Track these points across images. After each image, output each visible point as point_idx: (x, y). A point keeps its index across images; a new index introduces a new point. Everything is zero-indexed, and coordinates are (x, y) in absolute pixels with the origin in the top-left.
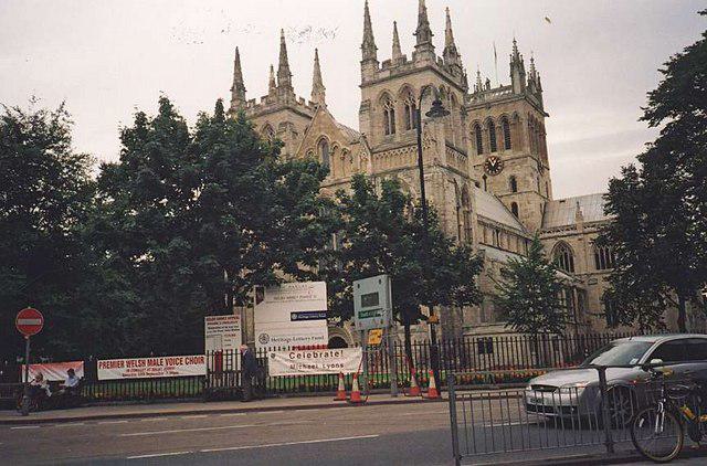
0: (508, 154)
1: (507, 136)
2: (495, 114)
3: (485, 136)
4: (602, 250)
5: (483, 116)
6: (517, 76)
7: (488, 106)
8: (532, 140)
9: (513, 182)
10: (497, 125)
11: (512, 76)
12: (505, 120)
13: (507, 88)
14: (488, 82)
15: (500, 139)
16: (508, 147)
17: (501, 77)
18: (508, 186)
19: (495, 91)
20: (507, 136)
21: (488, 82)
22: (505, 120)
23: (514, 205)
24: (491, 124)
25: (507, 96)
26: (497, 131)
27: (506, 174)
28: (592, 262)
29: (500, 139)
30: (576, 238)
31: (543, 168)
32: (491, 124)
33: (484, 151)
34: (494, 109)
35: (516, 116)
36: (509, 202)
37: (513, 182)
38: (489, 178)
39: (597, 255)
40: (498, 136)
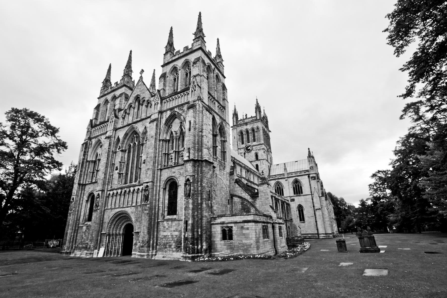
0: (254, 143)
1: (254, 136)
2: (249, 127)
3: (245, 137)
4: (296, 186)
5: (244, 128)
6: (258, 112)
7: (246, 124)
8: (264, 139)
9: (257, 156)
10: (250, 132)
11: (256, 112)
12: (253, 130)
13: (254, 117)
14: (246, 115)
15: (251, 137)
16: (254, 141)
17: (252, 113)
18: (254, 158)
19: (249, 118)
20: (254, 136)
21: (246, 115)
22: (253, 130)
23: (257, 166)
24: (247, 131)
25: (254, 120)
26: (250, 134)
27: (253, 153)
28: (292, 190)
29: (251, 137)
30: (285, 180)
31: (269, 150)
32: (247, 131)
33: (245, 142)
34: (248, 125)
35: (258, 128)
36: (255, 164)
37: (257, 156)
38: (246, 154)
39: (294, 188)
40: (250, 137)
